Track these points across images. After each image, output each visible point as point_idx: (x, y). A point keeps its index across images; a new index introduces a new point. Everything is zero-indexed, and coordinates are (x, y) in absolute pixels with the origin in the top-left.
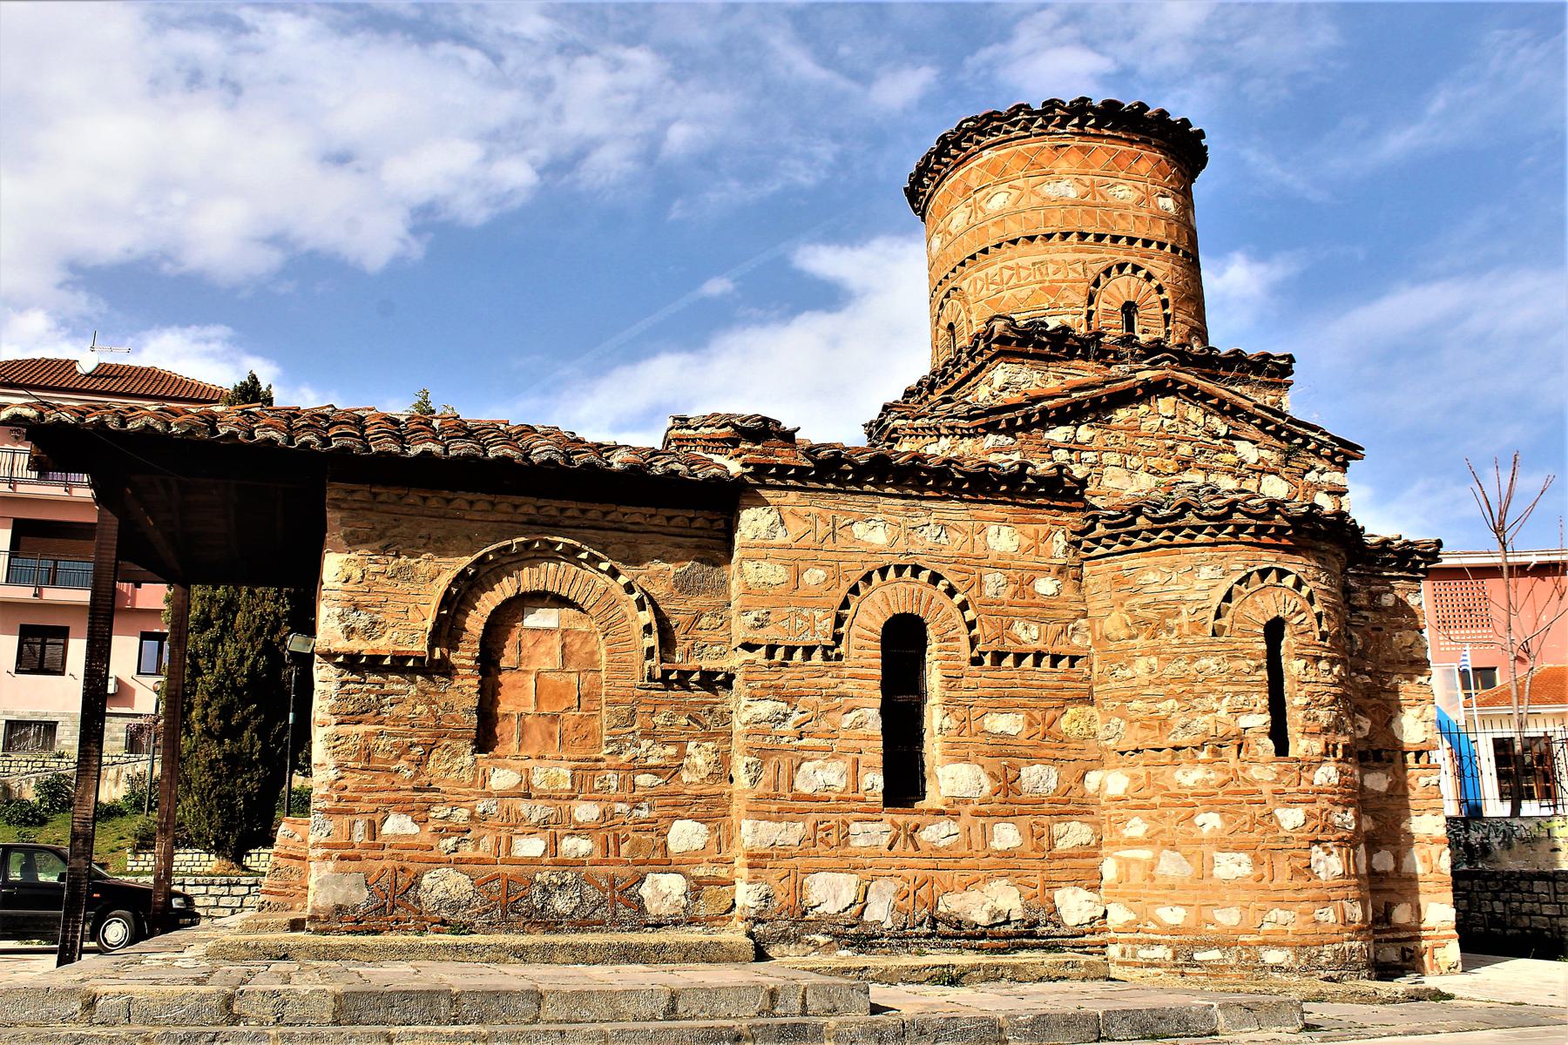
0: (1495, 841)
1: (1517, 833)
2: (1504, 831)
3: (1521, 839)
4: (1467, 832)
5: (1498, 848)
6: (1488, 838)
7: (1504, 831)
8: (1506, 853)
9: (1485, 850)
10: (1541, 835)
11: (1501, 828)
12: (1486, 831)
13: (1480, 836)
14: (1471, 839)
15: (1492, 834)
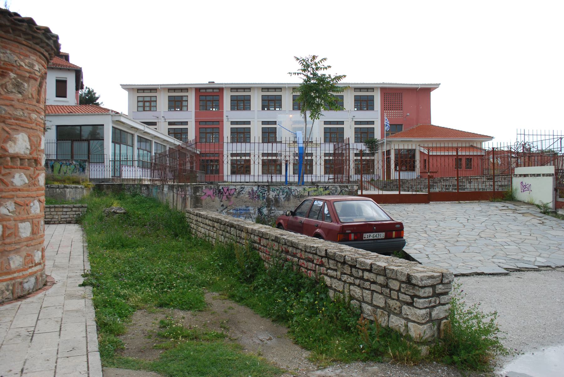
0: (282, 197)
1: (293, 193)
2: (287, 192)
3: (295, 196)
4: (269, 192)
5: (283, 200)
6: (278, 195)
7: (287, 192)
8: (286, 203)
9: (277, 200)
10: (305, 194)
11: (286, 191)
12: (278, 192)
13: (274, 194)
14: (270, 196)
15: (281, 194)
